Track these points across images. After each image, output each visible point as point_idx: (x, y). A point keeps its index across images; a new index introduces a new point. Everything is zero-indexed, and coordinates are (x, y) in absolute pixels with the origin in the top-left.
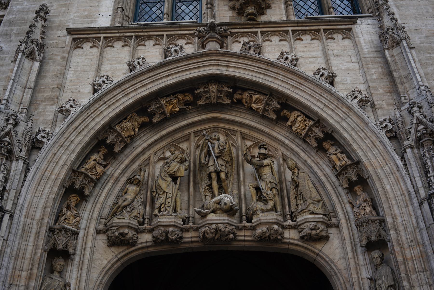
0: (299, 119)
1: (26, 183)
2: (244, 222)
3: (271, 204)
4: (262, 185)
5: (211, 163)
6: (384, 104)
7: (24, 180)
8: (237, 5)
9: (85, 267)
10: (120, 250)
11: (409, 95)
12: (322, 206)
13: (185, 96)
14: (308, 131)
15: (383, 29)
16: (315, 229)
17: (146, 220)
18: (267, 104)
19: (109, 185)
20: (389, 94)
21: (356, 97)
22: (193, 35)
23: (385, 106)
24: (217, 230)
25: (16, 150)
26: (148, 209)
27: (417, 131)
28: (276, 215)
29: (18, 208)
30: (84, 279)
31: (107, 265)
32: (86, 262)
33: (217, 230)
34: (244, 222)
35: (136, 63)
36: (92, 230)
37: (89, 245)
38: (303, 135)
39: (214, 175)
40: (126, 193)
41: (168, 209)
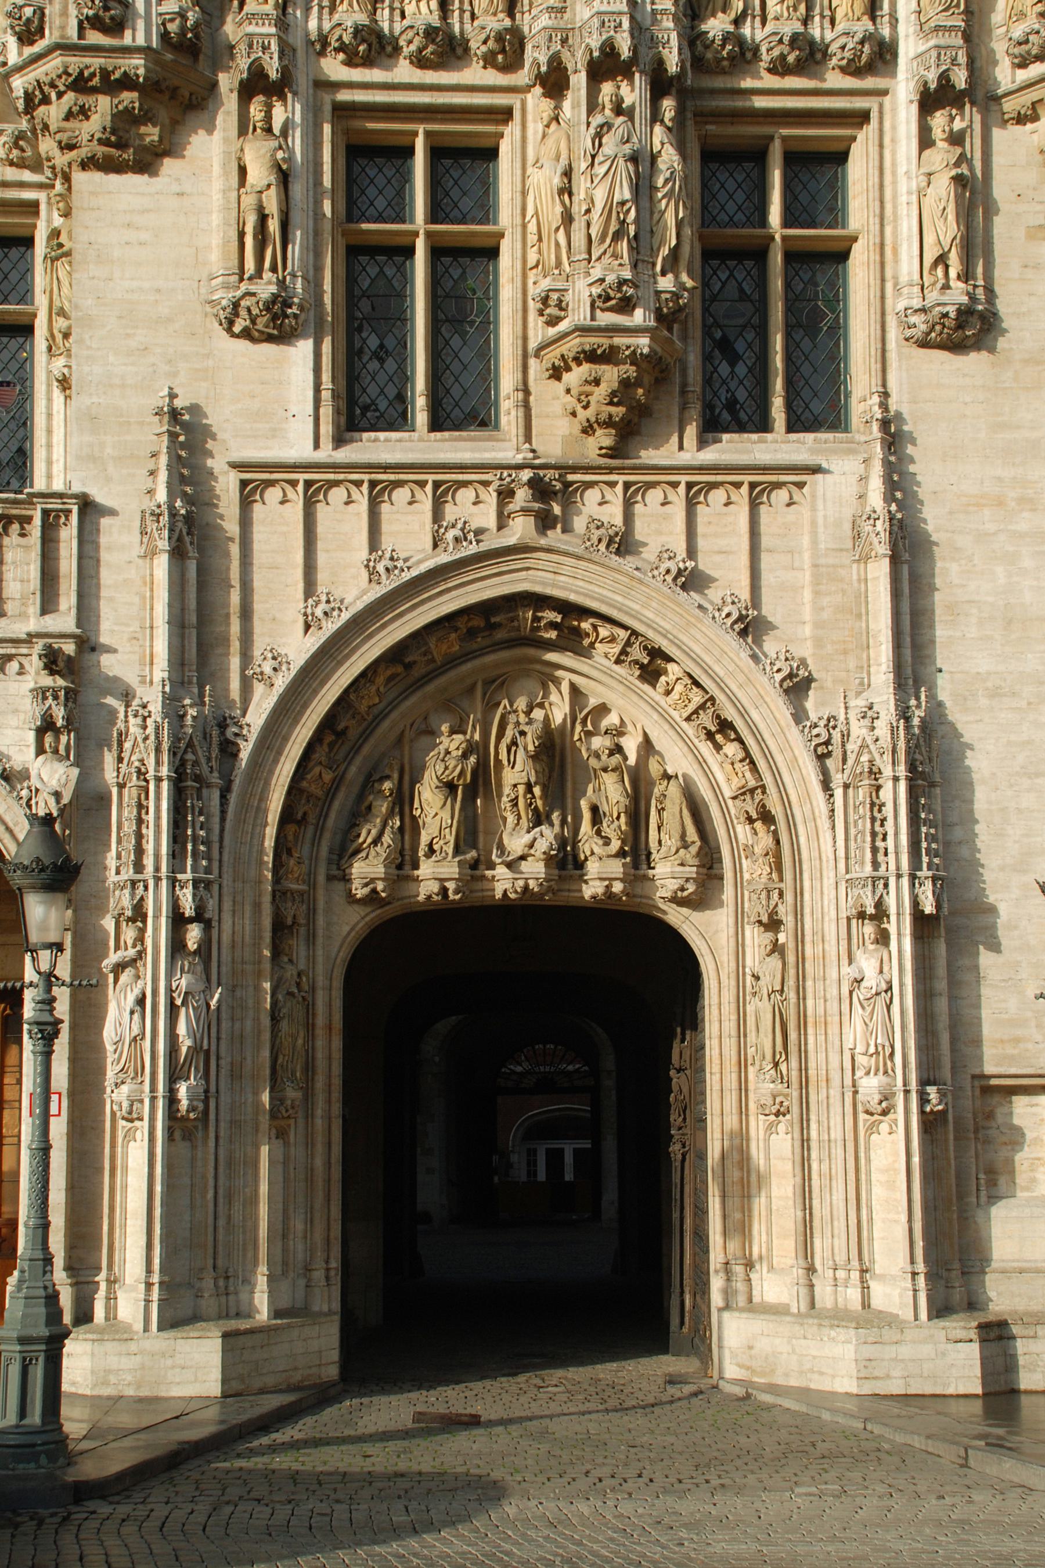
0: (679, 688)
1: (228, 825)
2: (570, 866)
3: (615, 845)
4: (604, 807)
5: (519, 766)
6: (830, 679)
7: (223, 819)
8: (582, 415)
9: (320, 940)
10: (369, 909)
11: (869, 674)
12: (701, 848)
13: (469, 620)
14: (692, 714)
15: (863, 505)
16: (682, 889)
17: (407, 858)
18: (624, 652)
19: (341, 795)
20: (842, 657)
21: (779, 671)
22: (486, 484)
23: (829, 684)
24: (526, 888)
25: (205, 769)
26: (407, 838)
27: (857, 761)
28: (624, 865)
29: (225, 869)
30: (320, 959)
31: (349, 933)
32: (320, 932)
33: (526, 888)
34: (570, 866)
35: (381, 568)
36: (321, 878)
37: (321, 904)
38: (685, 715)
39: (521, 789)
40: (369, 808)
41: (445, 848)
